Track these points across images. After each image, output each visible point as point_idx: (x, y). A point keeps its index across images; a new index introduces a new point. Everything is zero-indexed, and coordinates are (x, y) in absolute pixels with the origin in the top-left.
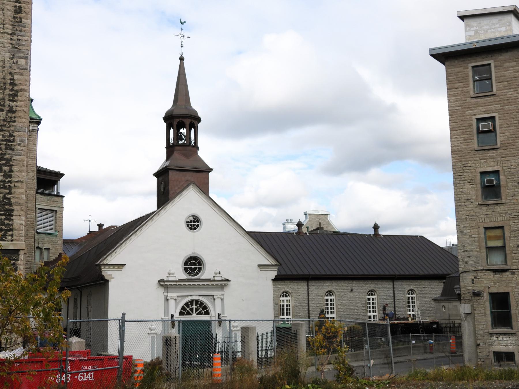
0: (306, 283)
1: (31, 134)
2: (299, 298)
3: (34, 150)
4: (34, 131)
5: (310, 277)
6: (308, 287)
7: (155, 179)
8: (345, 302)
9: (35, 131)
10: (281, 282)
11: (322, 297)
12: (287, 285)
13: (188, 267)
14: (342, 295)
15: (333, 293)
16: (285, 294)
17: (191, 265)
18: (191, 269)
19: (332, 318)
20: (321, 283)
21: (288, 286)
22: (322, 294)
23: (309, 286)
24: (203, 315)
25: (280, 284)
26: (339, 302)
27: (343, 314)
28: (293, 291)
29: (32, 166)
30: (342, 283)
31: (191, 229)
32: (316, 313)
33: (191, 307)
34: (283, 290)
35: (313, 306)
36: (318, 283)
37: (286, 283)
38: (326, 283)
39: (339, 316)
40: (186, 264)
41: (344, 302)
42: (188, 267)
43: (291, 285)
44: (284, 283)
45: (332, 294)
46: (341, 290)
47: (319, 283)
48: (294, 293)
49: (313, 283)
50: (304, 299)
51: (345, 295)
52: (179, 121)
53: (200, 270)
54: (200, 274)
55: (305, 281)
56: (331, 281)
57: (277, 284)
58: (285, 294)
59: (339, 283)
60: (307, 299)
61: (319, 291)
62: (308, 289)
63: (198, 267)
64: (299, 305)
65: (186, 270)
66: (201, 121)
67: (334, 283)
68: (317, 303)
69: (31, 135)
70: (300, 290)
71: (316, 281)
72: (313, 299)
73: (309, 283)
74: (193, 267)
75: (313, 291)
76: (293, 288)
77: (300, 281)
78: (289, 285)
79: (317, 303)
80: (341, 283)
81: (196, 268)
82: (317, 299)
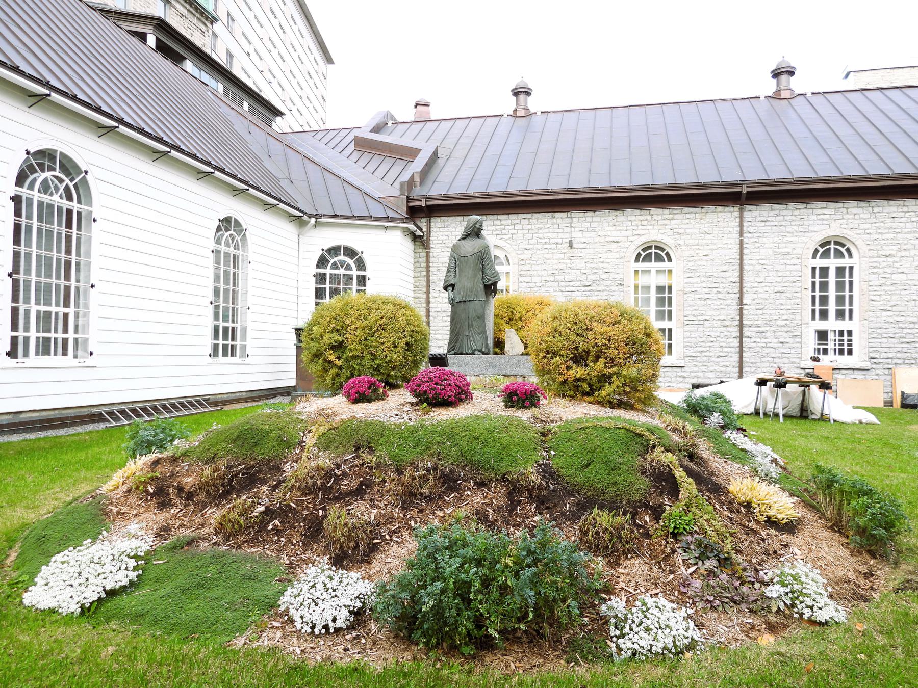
0: (737, 214)
2: (704, 263)
5: (745, 190)
6: (741, 226)
8: (904, 277)
10: (637, 212)
11: (797, 262)
12: (660, 222)
14: (887, 253)
15: (848, 245)
16: (653, 250)
19: (841, 333)
20: (796, 213)
21: (666, 225)
22: (798, 251)
23: (745, 224)
25: (633, 218)
26: (872, 277)
27: (891, 320)
28: (681, 242)
30: (894, 209)
32: (771, 315)
34: (644, 239)
35: (760, 290)
36: (783, 213)
37: (655, 217)
38: (819, 211)
39: (872, 325)
41: (895, 277)
43: (673, 222)
44: (649, 217)
45: (848, 250)
46: (887, 236)
47: (789, 212)
48: (684, 247)
49: (765, 213)
50: (725, 268)
51: (904, 253)
55: (730, 208)
56: (840, 205)
57: (623, 218)
58: (653, 250)
59: (876, 210)
60: (738, 267)
61: (785, 239)
62: (741, 234)
64: (704, 285)
67: (855, 210)
68: (778, 279)
70: (709, 236)
71: (776, 206)
72: (759, 268)
73: (745, 214)
75: (764, 240)
76: (682, 231)
77: (712, 209)
78: (667, 222)
79: (778, 279)
80: (887, 209)
82: (777, 267)
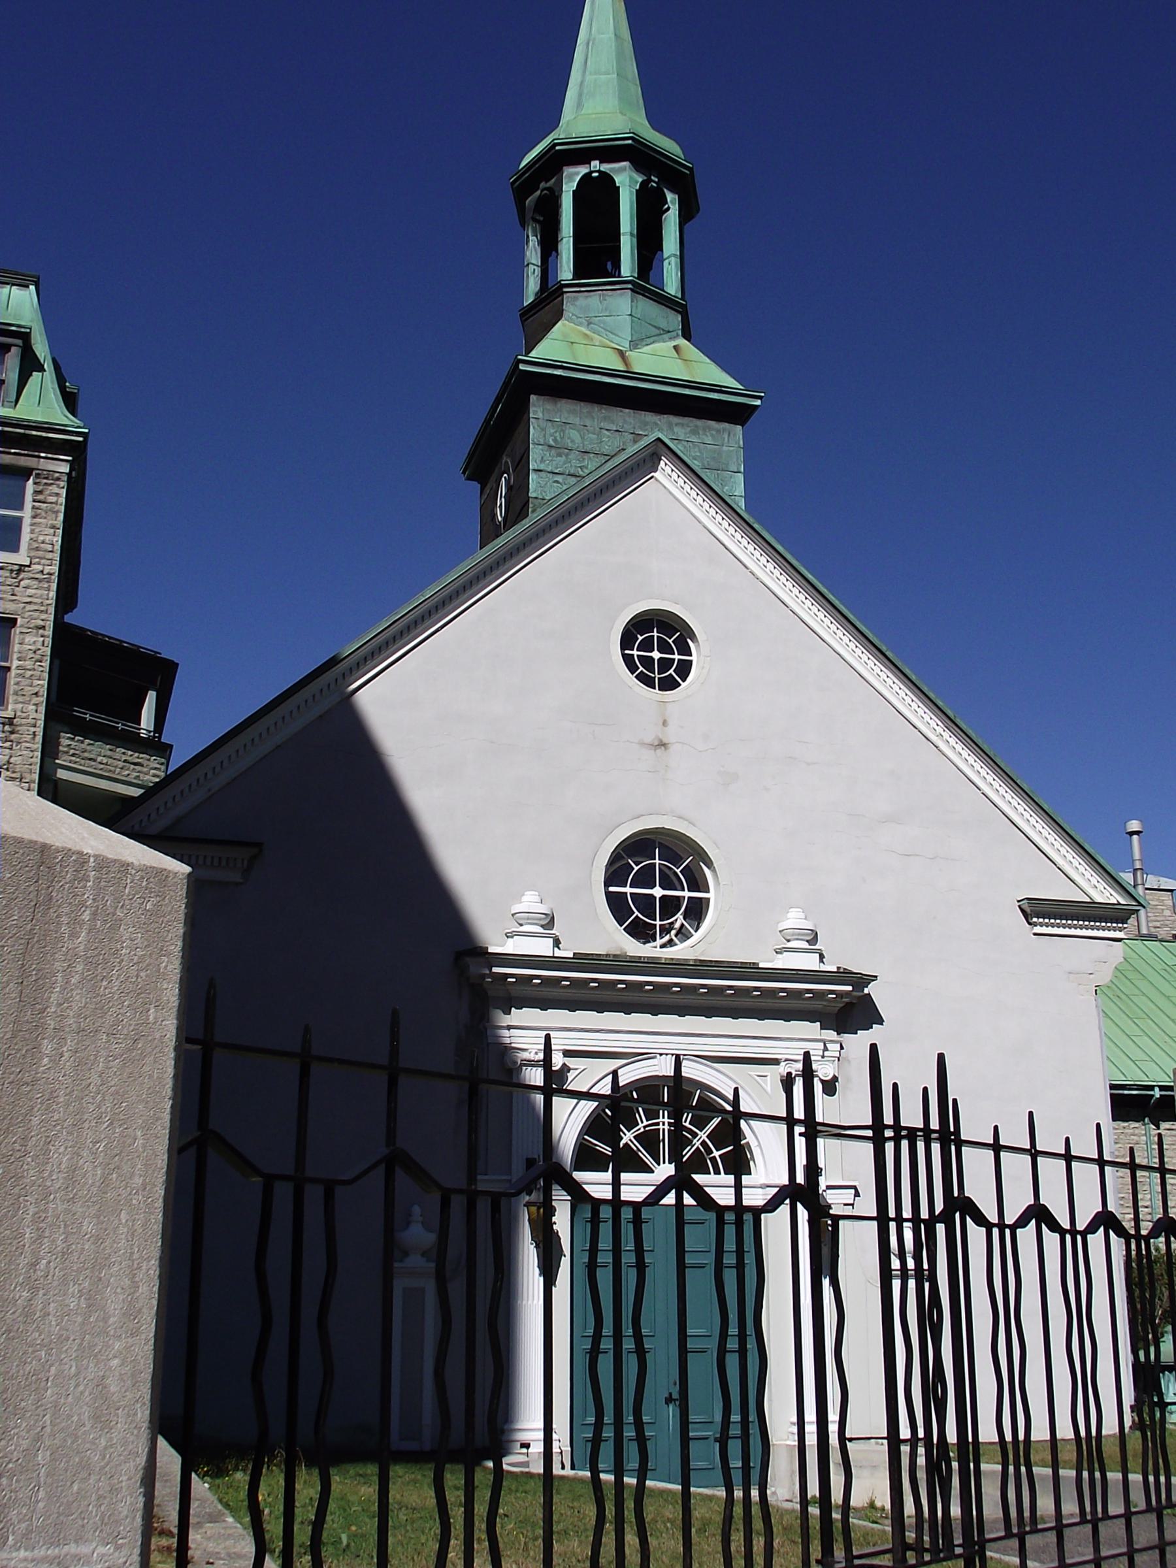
1: (40, 488)
3: (49, 547)
4: (57, 475)
7: (476, 486)
9: (58, 479)
13: (628, 890)
17: (645, 879)
18: (646, 903)
24: (717, 1172)
29: (36, 607)
31: (647, 681)
33: (643, 1124)
40: (615, 873)
42: (628, 890)
52: (592, 172)
53: (697, 912)
54: (697, 936)
63: (687, 894)
65: (618, 906)
66: (698, 210)
69: (41, 492)
74: (658, 892)
81: (678, 898)
